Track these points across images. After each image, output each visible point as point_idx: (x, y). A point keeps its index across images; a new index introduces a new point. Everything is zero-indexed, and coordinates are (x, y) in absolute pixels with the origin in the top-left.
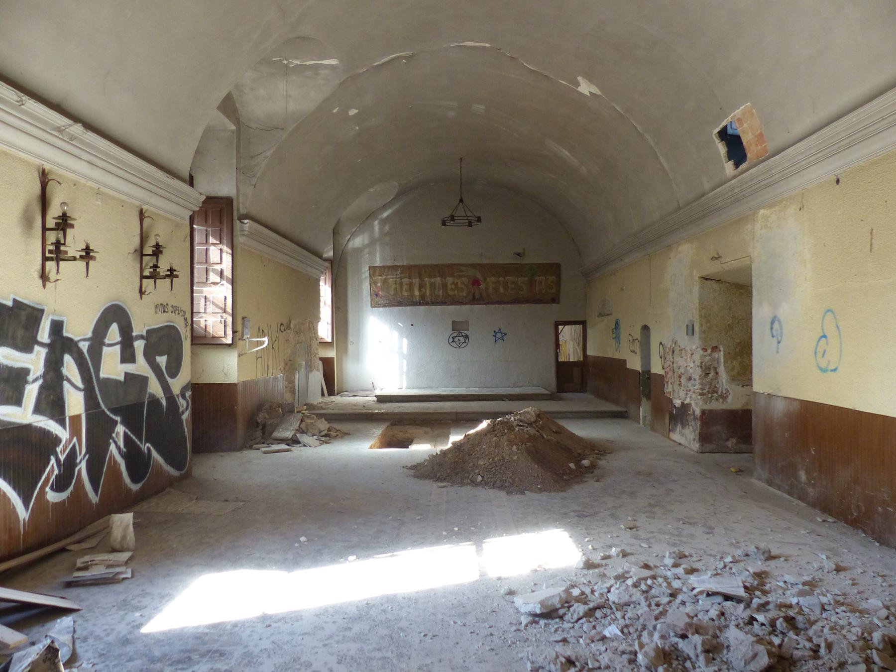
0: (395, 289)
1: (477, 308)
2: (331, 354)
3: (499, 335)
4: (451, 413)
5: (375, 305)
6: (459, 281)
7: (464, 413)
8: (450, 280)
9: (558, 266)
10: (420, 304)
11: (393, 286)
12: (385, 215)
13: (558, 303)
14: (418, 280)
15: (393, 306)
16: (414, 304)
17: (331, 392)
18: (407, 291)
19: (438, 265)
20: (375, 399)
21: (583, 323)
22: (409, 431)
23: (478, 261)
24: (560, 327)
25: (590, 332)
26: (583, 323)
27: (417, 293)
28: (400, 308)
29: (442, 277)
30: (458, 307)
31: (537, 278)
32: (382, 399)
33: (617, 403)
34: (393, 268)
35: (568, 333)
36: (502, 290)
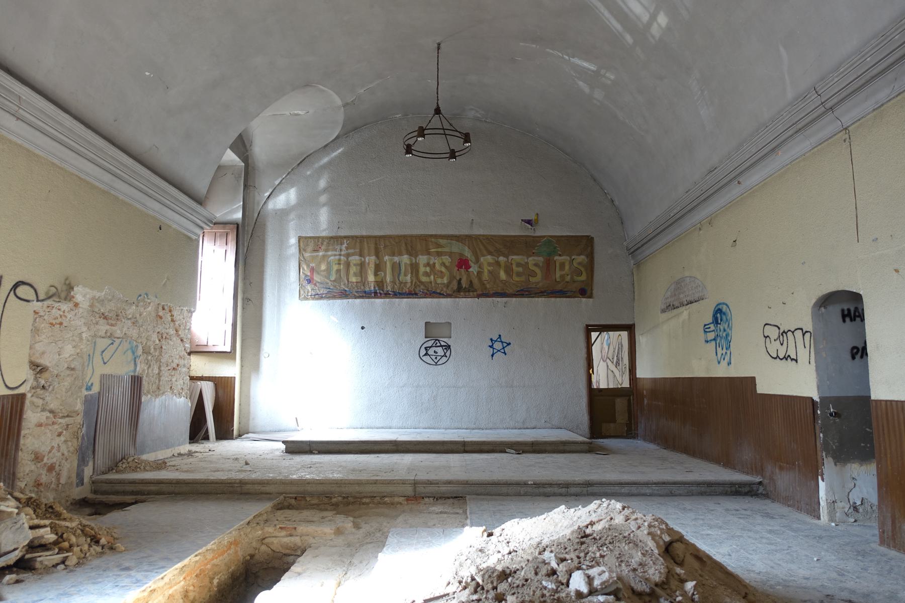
0: (338, 271)
1: (464, 302)
2: (229, 370)
3: (499, 346)
4: (404, 482)
5: (303, 297)
6: (437, 261)
7: (430, 483)
8: (422, 259)
9: (590, 240)
10: (376, 295)
11: (335, 267)
12: (326, 160)
13: (591, 297)
14: (373, 258)
15: (334, 297)
16: (366, 295)
17: (225, 433)
18: (355, 275)
19: (405, 236)
20: (283, 447)
21: (630, 328)
22: (302, 528)
23: (465, 231)
24: (594, 335)
25: (642, 341)
26: (630, 328)
27: (371, 278)
28: (345, 301)
29: (410, 255)
30: (435, 300)
31: (556, 258)
32: (295, 448)
33: (727, 462)
34: (335, 240)
35: (605, 345)
36: (503, 275)
